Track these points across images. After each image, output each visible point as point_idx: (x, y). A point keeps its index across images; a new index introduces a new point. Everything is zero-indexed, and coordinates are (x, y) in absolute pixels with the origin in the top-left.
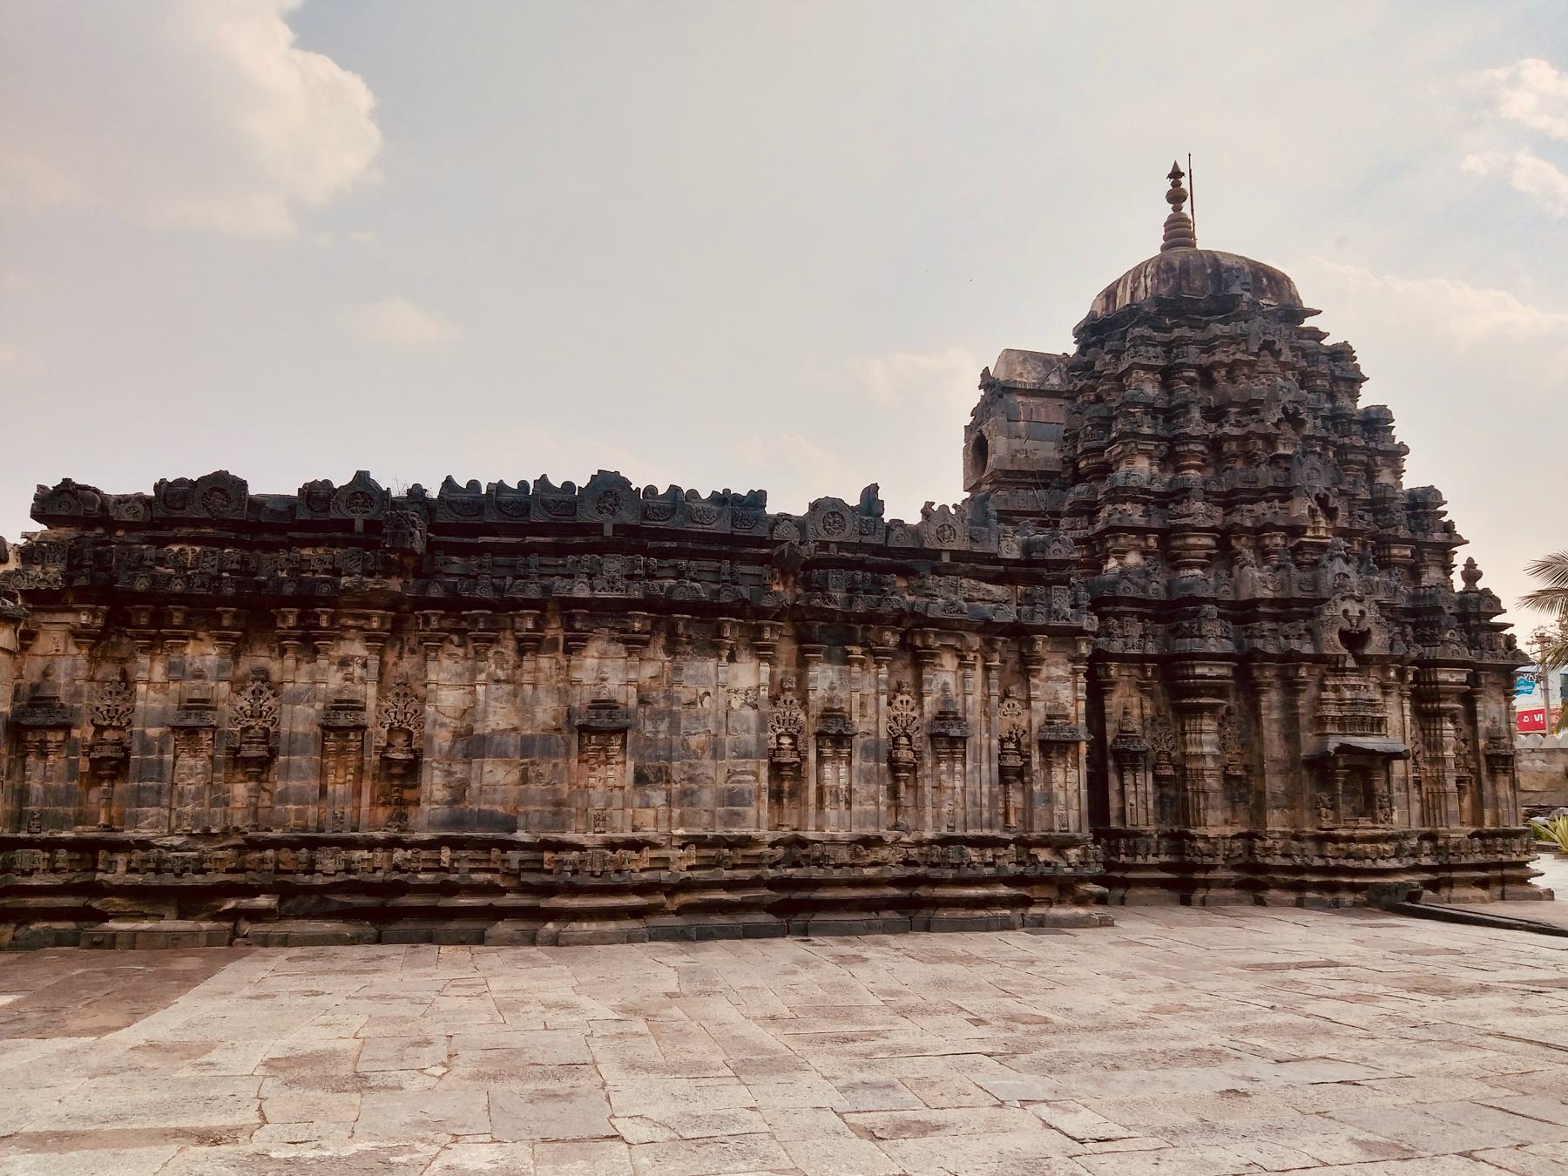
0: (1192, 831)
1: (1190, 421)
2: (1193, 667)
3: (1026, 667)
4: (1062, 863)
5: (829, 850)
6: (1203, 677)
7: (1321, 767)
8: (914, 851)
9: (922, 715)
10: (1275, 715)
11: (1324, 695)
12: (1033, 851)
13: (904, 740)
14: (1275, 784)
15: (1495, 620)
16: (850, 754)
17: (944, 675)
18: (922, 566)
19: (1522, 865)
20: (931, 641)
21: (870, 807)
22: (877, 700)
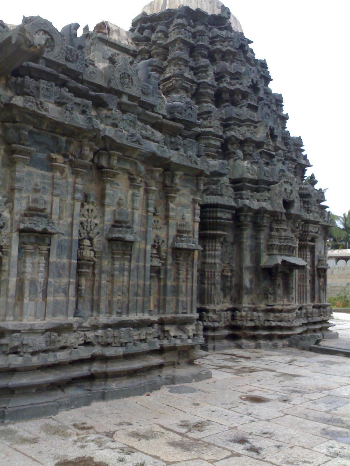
0: (208, 307)
1: (208, 75)
2: (216, 212)
3: (167, 193)
4: (185, 337)
5: (28, 339)
6: (221, 218)
7: (270, 273)
8: (90, 335)
9: (103, 222)
10: (262, 241)
11: (273, 233)
12: (167, 328)
13: (87, 242)
14: (247, 279)
15: (322, 204)
16: (49, 250)
17: (119, 191)
18: (112, 101)
19: (325, 321)
20: (115, 162)
21: (61, 298)
22: (73, 206)
